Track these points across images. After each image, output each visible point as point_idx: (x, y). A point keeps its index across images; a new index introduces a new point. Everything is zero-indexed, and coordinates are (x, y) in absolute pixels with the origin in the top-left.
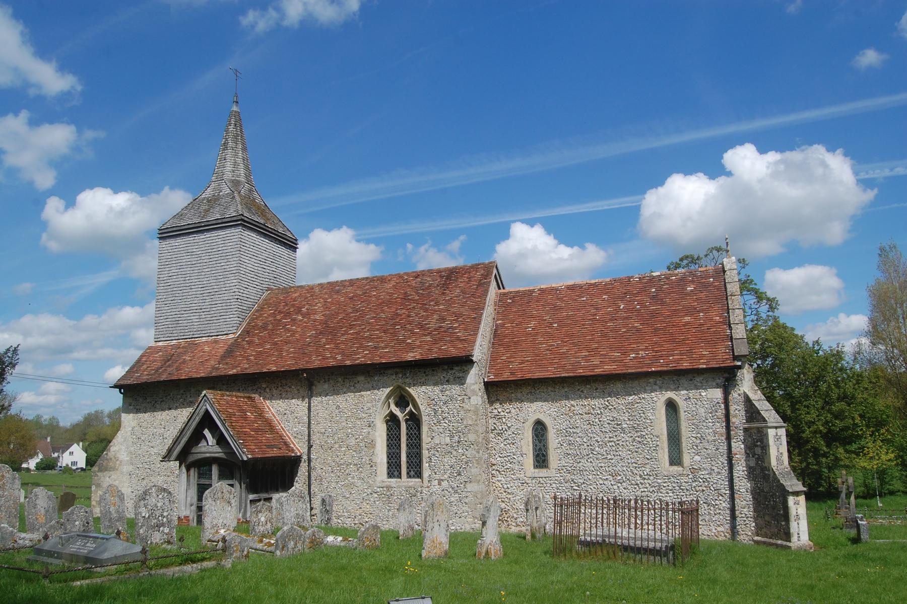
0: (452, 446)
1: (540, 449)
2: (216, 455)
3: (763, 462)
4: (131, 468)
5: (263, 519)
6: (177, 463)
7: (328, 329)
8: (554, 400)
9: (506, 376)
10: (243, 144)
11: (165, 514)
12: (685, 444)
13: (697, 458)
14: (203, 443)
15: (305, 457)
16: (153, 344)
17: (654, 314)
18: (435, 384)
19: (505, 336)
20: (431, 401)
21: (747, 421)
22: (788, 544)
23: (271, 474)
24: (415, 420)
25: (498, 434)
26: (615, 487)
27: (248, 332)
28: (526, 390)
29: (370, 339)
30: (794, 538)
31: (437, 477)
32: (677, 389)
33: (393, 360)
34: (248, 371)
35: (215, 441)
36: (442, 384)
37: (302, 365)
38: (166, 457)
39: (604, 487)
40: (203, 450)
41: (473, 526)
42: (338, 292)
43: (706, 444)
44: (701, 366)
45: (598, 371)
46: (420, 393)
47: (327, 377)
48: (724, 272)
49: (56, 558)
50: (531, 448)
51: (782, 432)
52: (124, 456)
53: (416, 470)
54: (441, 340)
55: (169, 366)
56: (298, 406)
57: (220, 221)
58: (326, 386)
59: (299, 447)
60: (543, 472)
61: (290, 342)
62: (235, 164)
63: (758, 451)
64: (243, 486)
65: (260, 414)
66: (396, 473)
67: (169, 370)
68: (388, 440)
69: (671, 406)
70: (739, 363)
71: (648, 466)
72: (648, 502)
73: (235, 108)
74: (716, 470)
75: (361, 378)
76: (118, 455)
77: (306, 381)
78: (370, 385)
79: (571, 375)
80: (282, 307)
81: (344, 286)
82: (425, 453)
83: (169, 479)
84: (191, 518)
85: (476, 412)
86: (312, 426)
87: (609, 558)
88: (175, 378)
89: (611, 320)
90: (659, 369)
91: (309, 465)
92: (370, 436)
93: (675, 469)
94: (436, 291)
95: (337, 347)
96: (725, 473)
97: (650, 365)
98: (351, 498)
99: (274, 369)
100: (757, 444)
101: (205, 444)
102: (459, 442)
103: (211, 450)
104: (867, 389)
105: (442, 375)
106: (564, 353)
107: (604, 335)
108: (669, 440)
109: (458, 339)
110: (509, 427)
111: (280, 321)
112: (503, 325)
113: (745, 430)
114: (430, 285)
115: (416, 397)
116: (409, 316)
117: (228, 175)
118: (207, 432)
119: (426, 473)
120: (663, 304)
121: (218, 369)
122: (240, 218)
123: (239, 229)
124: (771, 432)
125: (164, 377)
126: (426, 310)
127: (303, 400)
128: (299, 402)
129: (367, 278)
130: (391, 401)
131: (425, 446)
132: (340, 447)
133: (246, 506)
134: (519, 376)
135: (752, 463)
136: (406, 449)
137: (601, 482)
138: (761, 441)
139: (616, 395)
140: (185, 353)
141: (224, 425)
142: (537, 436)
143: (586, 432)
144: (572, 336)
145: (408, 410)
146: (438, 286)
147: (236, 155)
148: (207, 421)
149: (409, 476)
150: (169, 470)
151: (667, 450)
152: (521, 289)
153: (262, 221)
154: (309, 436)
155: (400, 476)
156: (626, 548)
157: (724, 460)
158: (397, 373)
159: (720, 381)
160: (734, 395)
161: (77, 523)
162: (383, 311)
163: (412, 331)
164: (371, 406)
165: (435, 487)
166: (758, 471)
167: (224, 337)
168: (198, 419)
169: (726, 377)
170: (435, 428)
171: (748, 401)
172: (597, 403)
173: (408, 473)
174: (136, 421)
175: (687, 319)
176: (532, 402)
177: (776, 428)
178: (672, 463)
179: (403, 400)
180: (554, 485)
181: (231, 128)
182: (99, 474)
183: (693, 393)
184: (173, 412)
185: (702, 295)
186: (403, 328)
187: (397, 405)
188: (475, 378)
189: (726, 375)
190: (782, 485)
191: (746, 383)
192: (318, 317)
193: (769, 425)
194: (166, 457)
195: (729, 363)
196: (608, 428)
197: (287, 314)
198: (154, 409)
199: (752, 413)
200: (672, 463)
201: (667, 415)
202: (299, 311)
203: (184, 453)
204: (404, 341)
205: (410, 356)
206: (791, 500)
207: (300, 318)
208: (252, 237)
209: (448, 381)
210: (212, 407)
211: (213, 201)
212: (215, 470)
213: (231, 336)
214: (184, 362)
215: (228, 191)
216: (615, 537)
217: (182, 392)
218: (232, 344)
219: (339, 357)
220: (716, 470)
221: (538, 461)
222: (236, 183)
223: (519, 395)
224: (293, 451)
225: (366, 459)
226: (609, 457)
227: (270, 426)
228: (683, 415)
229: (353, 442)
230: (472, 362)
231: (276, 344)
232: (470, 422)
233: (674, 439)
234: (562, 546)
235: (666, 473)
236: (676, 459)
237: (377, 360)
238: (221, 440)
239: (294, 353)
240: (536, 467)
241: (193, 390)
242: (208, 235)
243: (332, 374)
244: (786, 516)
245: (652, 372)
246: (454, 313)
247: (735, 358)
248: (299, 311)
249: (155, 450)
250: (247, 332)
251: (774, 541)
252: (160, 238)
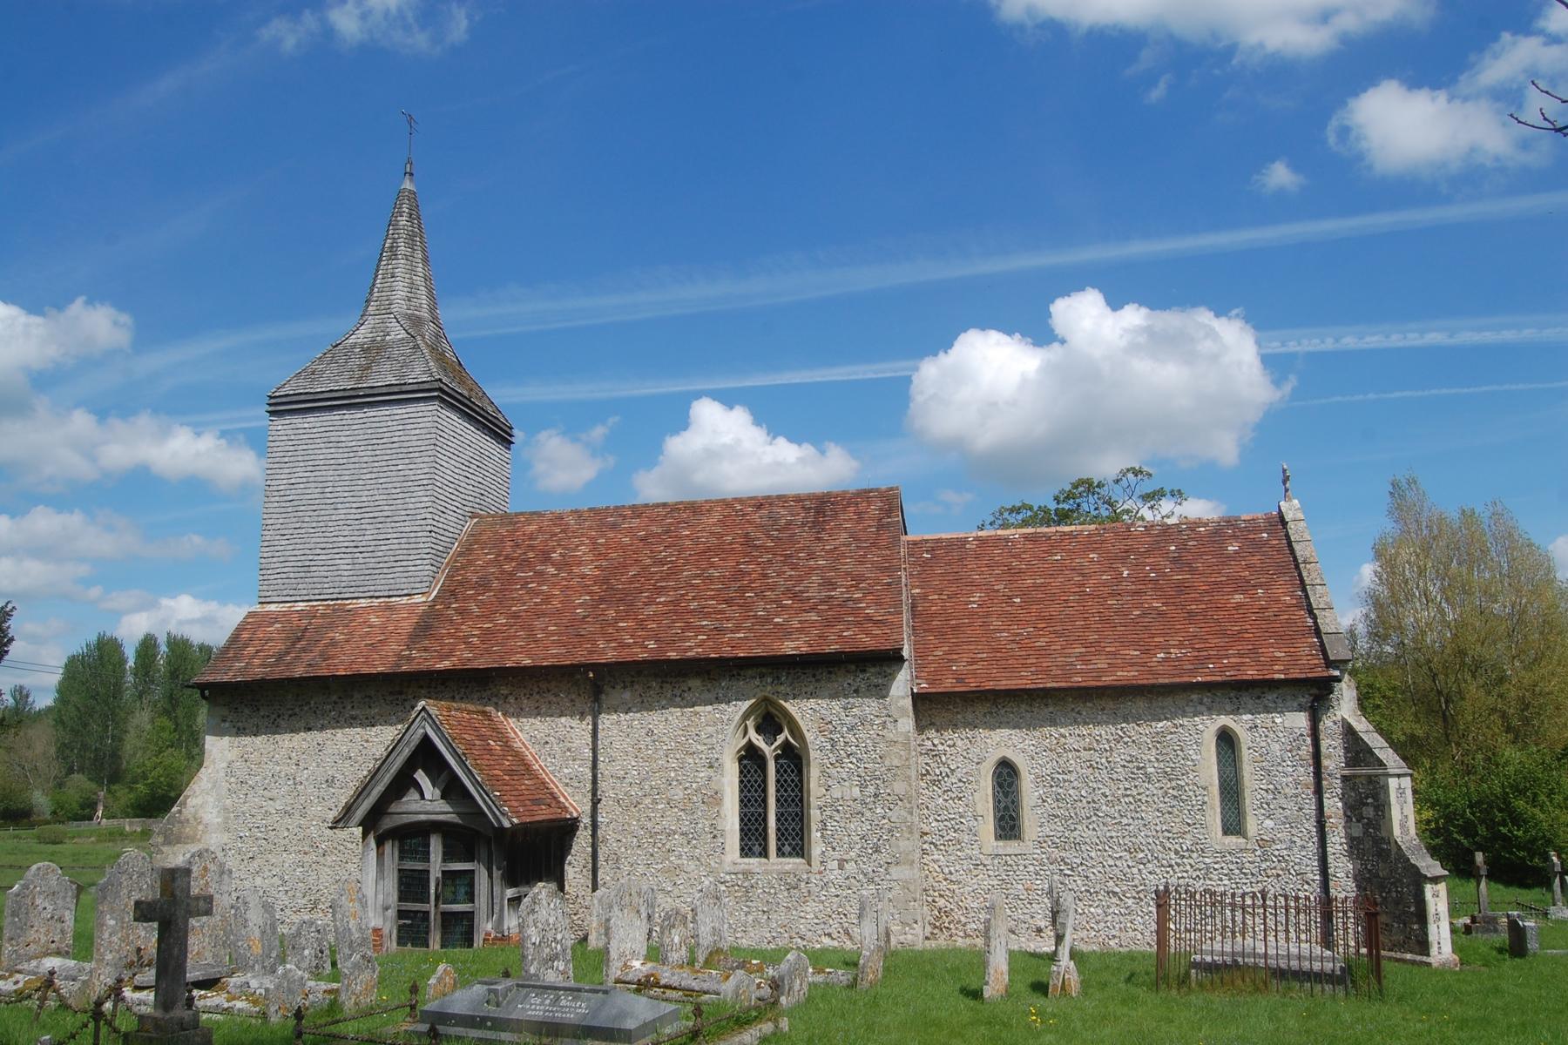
0: (864, 803)
1: (1006, 808)
2: (441, 817)
3: (1377, 828)
4: (225, 838)
5: (677, 939)
6: (358, 831)
7: (609, 592)
9: (948, 685)
10: (423, 251)
11: (559, 937)
12: (1250, 800)
13: (1269, 823)
14: (413, 795)
15: (586, 820)
16: (257, 608)
17: (1181, 588)
18: (833, 696)
19: (933, 616)
20: (825, 725)
21: (1348, 765)
22: (1424, 959)
23: (537, 851)
24: (793, 758)
25: (933, 782)
26: (1135, 870)
27: (453, 593)
28: (981, 709)
29: (702, 613)
30: (1434, 950)
31: (836, 855)
32: (1236, 711)
33: (758, 652)
34: (475, 665)
35: (438, 792)
36: (846, 696)
37: (580, 656)
38: (337, 823)
39: (1117, 871)
40: (414, 807)
41: (902, 938)
42: (614, 526)
43: (1282, 801)
44: (1277, 676)
45: (1107, 680)
46: (807, 712)
47: (628, 679)
48: (1284, 523)
49: (490, 1029)
50: (991, 805)
51: (1407, 783)
52: (211, 816)
53: (795, 840)
54: (838, 620)
55: (304, 650)
56: (575, 729)
57: (396, 389)
58: (627, 695)
59: (576, 804)
60: (1012, 847)
61: (544, 614)
62: (412, 287)
63: (1369, 812)
64: (497, 874)
65: (507, 744)
66: (757, 849)
67: (307, 657)
68: (741, 791)
69: (1226, 740)
70: (1337, 673)
71: (1188, 836)
72: (1297, 899)
73: (407, 185)
74: (1299, 843)
75: (695, 683)
76: (201, 813)
77: (590, 685)
78: (711, 696)
79: (1063, 685)
80: (504, 552)
81: (624, 517)
82: (815, 815)
83: (306, 858)
84: (386, 931)
85: (906, 745)
86: (601, 766)
87: (1257, 989)
88: (325, 672)
89: (1112, 595)
90: (1209, 679)
91: (594, 835)
92: (713, 785)
93: (1233, 840)
94: (804, 535)
95: (641, 624)
96: (1313, 847)
97: (1193, 672)
98: (676, 892)
99: (527, 662)
100: (1366, 801)
101: (417, 796)
102: (876, 796)
103: (429, 807)
104: (1378, 706)
105: (846, 681)
106: (1041, 648)
107: (1106, 621)
108: (1221, 793)
109: (869, 618)
110: (953, 771)
111: (512, 574)
112: (924, 597)
113: (1345, 779)
114: (789, 523)
115: (797, 717)
116: (765, 576)
117: (400, 306)
118: (420, 776)
119: (817, 848)
120: (1193, 571)
121: (409, 659)
122: (436, 385)
123: (434, 406)
124: (1393, 782)
125: (299, 671)
126: (794, 567)
127: (582, 719)
128: (575, 722)
129: (664, 505)
130: (750, 723)
131: (814, 802)
132: (655, 802)
133: (502, 910)
134: (972, 685)
135: (1357, 831)
136: (776, 805)
137: (1111, 862)
138: (1375, 797)
139: (1137, 719)
140: (331, 626)
141: (462, 763)
142: (1000, 785)
143: (1085, 780)
144: (1050, 619)
145: (780, 739)
146: (803, 525)
147: (412, 271)
148: (426, 755)
149: (781, 853)
150: (308, 842)
151: (1219, 810)
152: (944, 536)
153: (466, 393)
154: (595, 781)
155: (764, 853)
156: (1281, 974)
157: (1311, 826)
158: (762, 676)
159: (1305, 700)
160: (1328, 723)
161: (306, 952)
162: (712, 565)
163: (777, 601)
164: (718, 729)
165: (834, 874)
166: (1368, 844)
167: (405, 600)
168: (407, 752)
170: (833, 771)
171: (1349, 732)
172: (1104, 732)
173: (779, 849)
174: (236, 751)
175: (1238, 598)
176: (993, 728)
177: (1399, 776)
178: (1227, 831)
179: (770, 722)
180: (1031, 868)
181: (403, 221)
182: (165, 849)
183: (1260, 719)
184: (316, 736)
185: (1255, 560)
186: (760, 595)
187: (758, 730)
188: (902, 684)
189: (1314, 691)
190: (1414, 866)
191: (1345, 705)
192: (586, 571)
193: (1391, 771)
194: (337, 823)
195: (1320, 672)
196: (1121, 773)
197: (524, 563)
198: (274, 728)
199: (1357, 751)
200: (1227, 831)
201: (1218, 754)
202: (546, 558)
203: (377, 817)
204: (768, 620)
205: (789, 647)
206: (1429, 889)
207: (552, 570)
208: (453, 422)
209: (856, 691)
210: (437, 729)
211: (375, 351)
212: (436, 846)
213: (419, 599)
214: (333, 643)
215: (403, 335)
216: (1266, 955)
217: (334, 698)
218: (424, 613)
219: (652, 645)
220: (1299, 843)
221: (1002, 828)
222: (416, 321)
223: (970, 717)
224: (565, 809)
225: (704, 824)
226: (1125, 821)
227: (523, 767)
228: (1246, 755)
229: (678, 793)
230: (901, 660)
231: (516, 616)
232: (896, 762)
233: (1231, 792)
234: (1166, 973)
235: (1218, 848)
236: (1233, 825)
237: (727, 652)
238: (452, 789)
239: (560, 634)
240: (999, 837)
241: (357, 696)
242: (371, 412)
243: (639, 673)
244: (1422, 916)
245: (1198, 683)
246: (848, 574)
247: (1330, 664)
248: (546, 558)
249: (278, 805)
250: (450, 592)
251: (1399, 955)
252: (272, 413)
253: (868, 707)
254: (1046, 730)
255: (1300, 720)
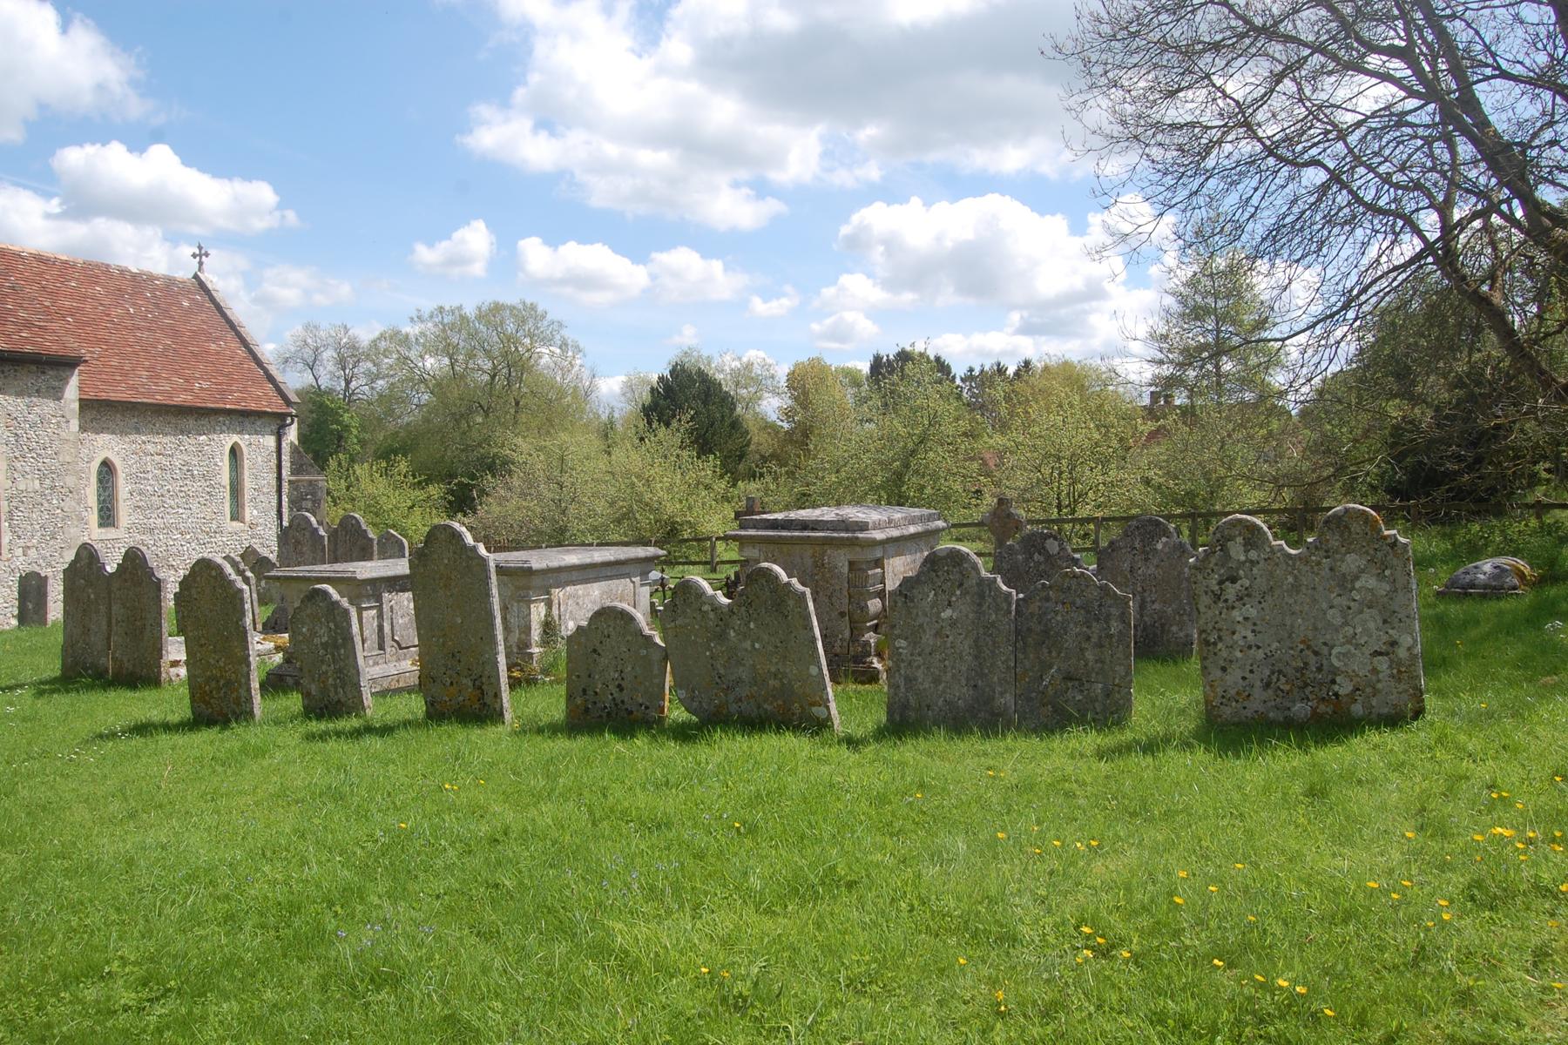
8: (123, 433)
12: (248, 494)
18: (19, 394)
32: (241, 432)
102: (52, 488)
159: (274, 427)
169: (278, 423)
178: (232, 519)
188: (72, 390)
200: (232, 519)
236: (236, 516)
240: (101, 525)
253: (47, 406)
254: (132, 437)
255: (270, 441)
